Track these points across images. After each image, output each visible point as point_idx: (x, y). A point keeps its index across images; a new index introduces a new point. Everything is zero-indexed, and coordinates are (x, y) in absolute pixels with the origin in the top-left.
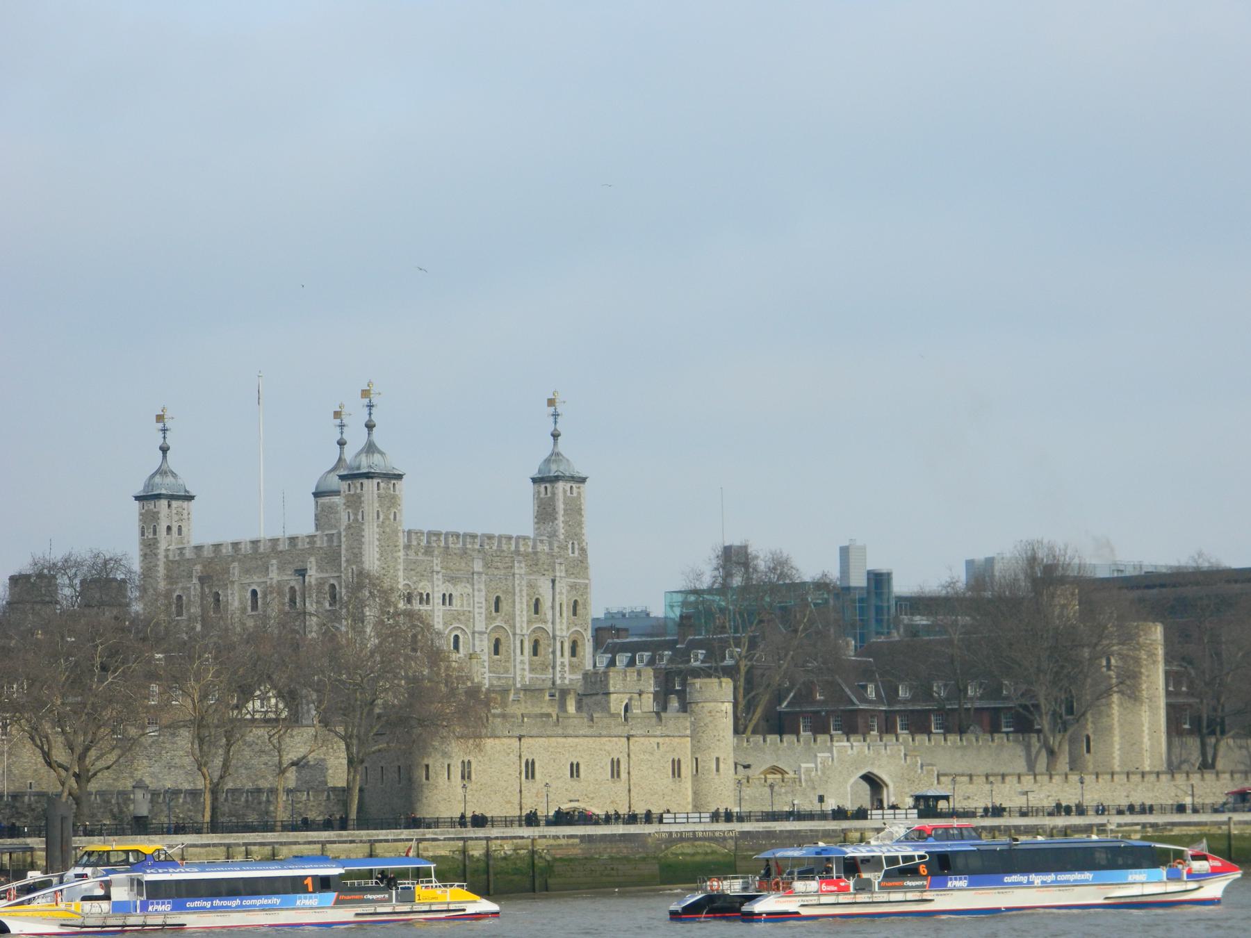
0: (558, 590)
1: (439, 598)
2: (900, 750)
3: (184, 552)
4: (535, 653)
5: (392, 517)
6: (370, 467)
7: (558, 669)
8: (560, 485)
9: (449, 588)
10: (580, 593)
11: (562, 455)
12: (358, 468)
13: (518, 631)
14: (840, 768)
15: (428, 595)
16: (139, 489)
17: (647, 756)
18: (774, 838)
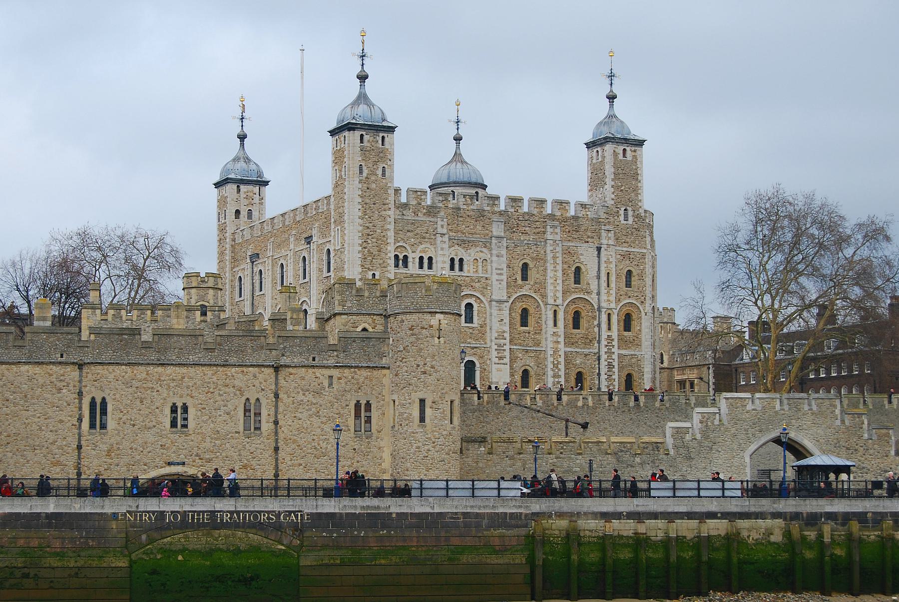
0: (603, 258)
1: (444, 262)
3: (244, 233)
4: (576, 325)
5: (380, 172)
7: (604, 342)
8: (609, 147)
9: (459, 252)
10: (636, 263)
11: (616, 117)
13: (551, 301)
14: (733, 430)
15: (430, 259)
16: (217, 179)
17: (310, 397)
18: (383, 528)
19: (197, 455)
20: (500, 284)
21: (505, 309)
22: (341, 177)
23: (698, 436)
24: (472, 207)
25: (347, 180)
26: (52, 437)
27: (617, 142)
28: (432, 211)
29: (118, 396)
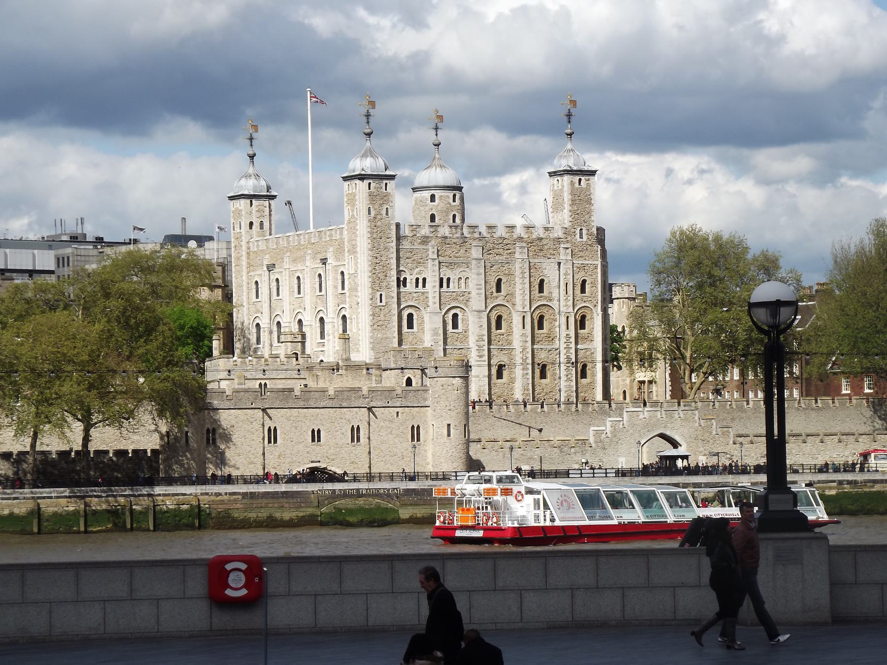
1: (435, 281)
2: (695, 415)
3: (260, 243)
5: (384, 212)
6: (363, 170)
8: (567, 179)
12: (354, 171)
14: (631, 431)
19: (327, 457)
20: (480, 297)
21: (484, 317)
22: (353, 215)
23: (609, 435)
24: (456, 236)
25: (358, 219)
26: (248, 449)
27: (574, 174)
28: (425, 240)
29: (283, 425)
